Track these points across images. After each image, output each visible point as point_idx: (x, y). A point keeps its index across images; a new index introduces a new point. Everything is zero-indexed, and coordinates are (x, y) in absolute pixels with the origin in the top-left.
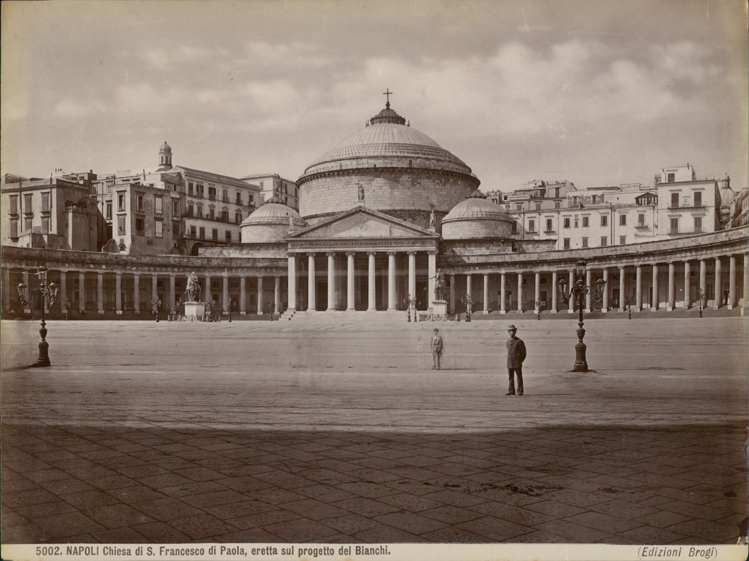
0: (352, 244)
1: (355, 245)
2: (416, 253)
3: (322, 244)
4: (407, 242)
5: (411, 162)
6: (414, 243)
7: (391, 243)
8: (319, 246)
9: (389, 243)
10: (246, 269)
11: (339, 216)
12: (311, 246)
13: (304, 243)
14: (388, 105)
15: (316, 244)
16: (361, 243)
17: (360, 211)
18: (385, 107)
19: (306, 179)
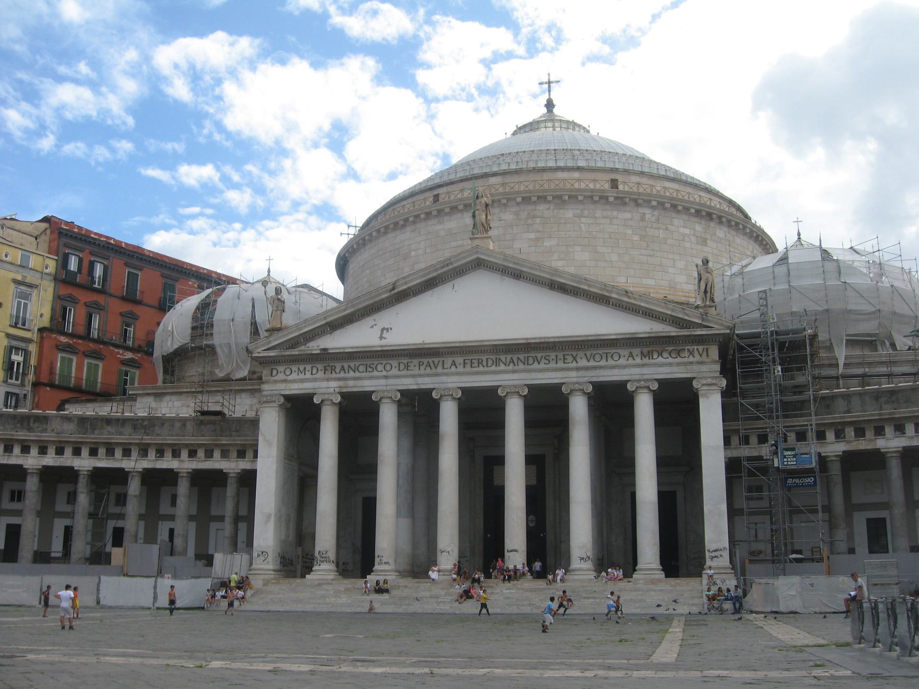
0: (454, 363)
1: (460, 369)
2: (655, 386)
3: (361, 368)
4: (624, 352)
5: (614, 184)
6: (649, 355)
7: (575, 359)
8: (352, 374)
9: (570, 359)
12: (328, 375)
13: (308, 367)
14: (550, 105)
15: (343, 369)
16: (480, 362)
17: (478, 264)
18: (545, 110)
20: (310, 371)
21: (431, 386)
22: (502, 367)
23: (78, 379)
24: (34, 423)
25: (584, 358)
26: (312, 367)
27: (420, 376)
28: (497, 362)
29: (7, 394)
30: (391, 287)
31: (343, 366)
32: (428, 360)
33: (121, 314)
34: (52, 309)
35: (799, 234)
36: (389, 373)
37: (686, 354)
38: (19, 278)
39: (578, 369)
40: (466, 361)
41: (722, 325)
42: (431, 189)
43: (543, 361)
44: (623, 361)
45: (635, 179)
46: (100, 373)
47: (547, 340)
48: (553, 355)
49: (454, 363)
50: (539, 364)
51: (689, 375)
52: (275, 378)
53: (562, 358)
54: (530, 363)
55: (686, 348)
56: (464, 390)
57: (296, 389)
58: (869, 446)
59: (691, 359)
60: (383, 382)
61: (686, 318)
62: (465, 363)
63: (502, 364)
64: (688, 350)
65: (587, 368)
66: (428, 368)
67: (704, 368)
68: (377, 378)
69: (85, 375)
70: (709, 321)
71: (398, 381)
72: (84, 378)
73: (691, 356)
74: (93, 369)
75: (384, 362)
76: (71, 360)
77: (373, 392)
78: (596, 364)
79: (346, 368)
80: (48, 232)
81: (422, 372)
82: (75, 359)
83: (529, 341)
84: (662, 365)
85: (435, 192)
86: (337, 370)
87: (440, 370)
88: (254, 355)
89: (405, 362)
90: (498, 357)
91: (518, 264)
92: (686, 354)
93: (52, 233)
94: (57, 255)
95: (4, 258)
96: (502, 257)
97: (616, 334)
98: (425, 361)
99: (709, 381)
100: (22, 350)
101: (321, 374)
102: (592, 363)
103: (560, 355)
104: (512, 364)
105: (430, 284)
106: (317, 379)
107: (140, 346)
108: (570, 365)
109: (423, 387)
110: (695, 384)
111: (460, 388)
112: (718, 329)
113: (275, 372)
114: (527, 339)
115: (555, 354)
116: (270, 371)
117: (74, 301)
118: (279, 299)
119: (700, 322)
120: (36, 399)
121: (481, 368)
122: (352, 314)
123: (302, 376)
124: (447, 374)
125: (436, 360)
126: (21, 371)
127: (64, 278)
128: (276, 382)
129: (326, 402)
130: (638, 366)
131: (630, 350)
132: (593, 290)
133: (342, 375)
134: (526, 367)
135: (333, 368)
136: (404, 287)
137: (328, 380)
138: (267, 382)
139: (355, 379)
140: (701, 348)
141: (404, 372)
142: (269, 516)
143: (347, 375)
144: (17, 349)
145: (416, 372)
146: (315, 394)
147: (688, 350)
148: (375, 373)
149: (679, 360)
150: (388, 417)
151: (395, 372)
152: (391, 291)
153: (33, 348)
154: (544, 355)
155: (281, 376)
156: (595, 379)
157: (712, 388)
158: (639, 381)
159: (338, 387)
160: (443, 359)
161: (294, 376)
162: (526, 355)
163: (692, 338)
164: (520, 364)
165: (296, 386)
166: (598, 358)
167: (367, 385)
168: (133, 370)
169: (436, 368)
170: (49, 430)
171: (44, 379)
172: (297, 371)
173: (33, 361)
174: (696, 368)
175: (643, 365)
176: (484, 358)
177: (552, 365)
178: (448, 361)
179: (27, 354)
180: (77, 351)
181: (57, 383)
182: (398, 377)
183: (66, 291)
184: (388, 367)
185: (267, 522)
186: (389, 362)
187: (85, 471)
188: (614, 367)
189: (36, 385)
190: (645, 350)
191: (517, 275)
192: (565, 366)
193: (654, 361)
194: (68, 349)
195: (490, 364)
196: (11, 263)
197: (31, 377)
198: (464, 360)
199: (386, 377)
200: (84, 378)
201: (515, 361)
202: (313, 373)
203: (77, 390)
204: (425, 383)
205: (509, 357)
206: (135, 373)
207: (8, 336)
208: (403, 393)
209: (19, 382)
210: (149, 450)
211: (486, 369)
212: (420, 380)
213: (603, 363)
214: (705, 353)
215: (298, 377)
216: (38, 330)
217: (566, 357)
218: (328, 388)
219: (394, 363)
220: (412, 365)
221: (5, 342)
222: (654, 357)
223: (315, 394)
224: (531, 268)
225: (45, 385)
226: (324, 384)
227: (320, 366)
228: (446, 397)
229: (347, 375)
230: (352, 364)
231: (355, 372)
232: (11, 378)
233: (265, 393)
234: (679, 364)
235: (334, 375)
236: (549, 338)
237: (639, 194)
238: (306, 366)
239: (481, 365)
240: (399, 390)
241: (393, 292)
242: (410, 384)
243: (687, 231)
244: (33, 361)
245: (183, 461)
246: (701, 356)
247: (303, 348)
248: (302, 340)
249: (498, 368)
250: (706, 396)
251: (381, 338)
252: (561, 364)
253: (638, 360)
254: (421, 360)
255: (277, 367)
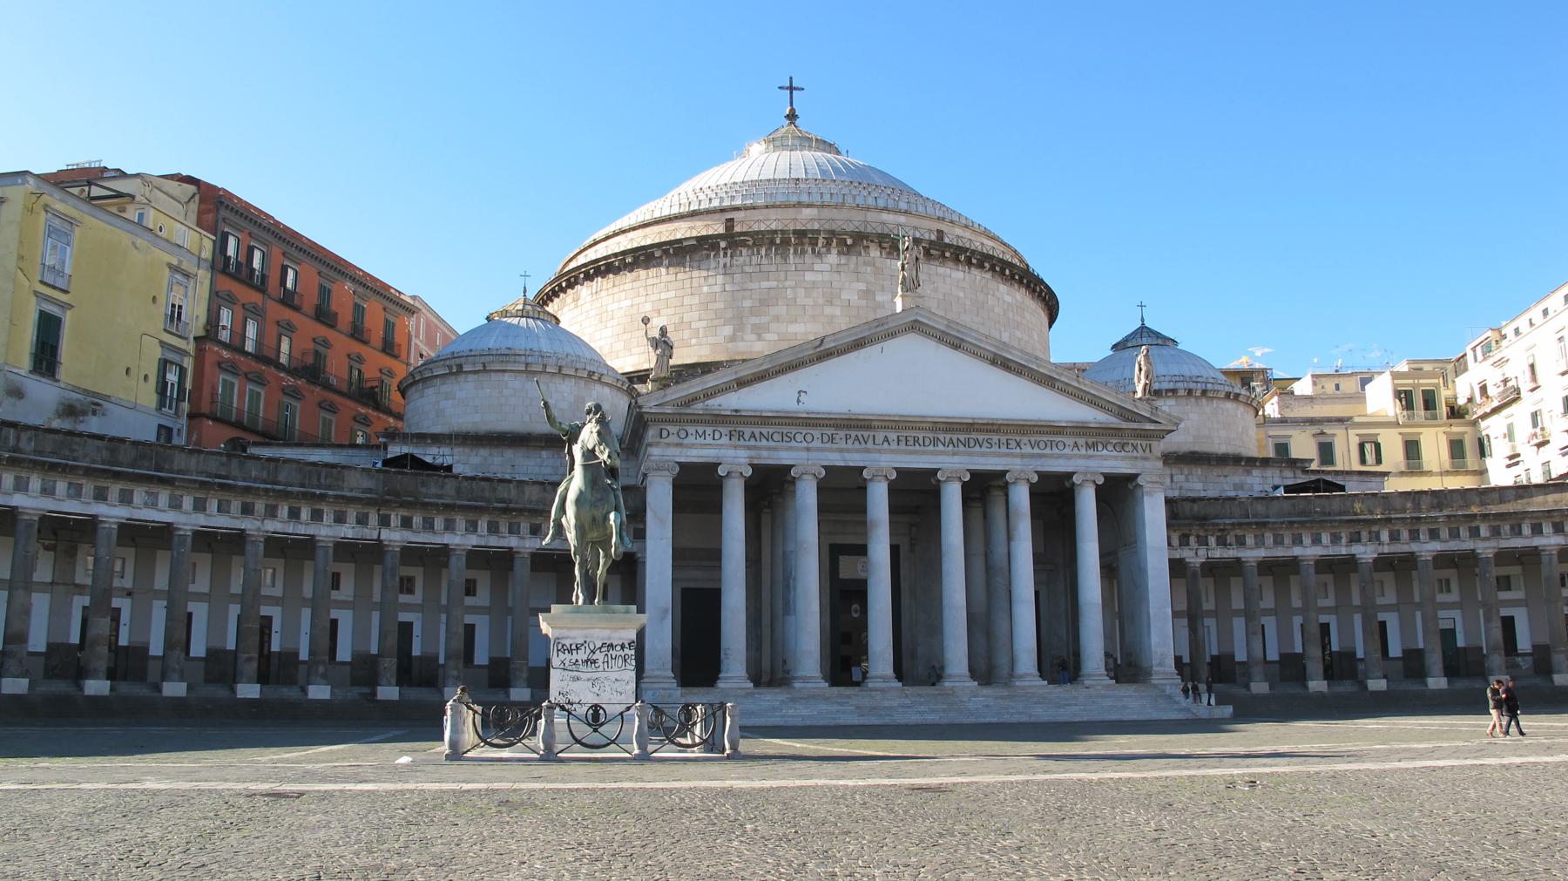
1: (894, 446)
2: (1101, 481)
3: (776, 437)
4: (1069, 441)
6: (1094, 446)
7: (1018, 444)
8: (764, 442)
9: (1013, 444)
10: (526, 514)
11: (745, 371)
12: (735, 441)
13: (709, 430)
16: (916, 440)
17: (916, 327)
19: (567, 280)
20: (712, 435)
21: (861, 464)
22: (941, 447)
23: (240, 411)
24: (326, 479)
25: (1028, 444)
26: (714, 431)
27: (848, 451)
28: (935, 442)
29: (160, 426)
30: (818, 343)
31: (753, 432)
32: (856, 433)
33: (278, 323)
34: (208, 310)
35: (1143, 320)
36: (810, 445)
37: (1130, 448)
38: (175, 262)
39: (1023, 456)
40: (900, 438)
41: (1170, 421)
42: (723, 211)
43: (985, 444)
44: (1067, 451)
45: (958, 231)
46: (262, 406)
47: (995, 422)
48: (995, 438)
49: (886, 439)
50: (981, 447)
51: (1133, 471)
52: (662, 440)
53: (1005, 442)
54: (972, 444)
55: (1130, 442)
56: (899, 471)
57: (697, 453)
58: (1290, 554)
59: (1135, 453)
60: (804, 455)
61: (1136, 410)
62: (899, 441)
63: (940, 444)
64: (1132, 444)
65: (1032, 456)
66: (857, 442)
67: (1147, 464)
68: (798, 449)
69: (246, 407)
70: (1158, 417)
71: (822, 455)
72: (246, 409)
73: (1135, 451)
74: (255, 397)
75: (804, 432)
76: (232, 384)
77: (793, 466)
78: (1040, 451)
79: (757, 435)
80: (197, 197)
81: (850, 445)
82: (236, 382)
83: (976, 421)
84: (1106, 458)
85: (729, 215)
86: (747, 436)
87: (870, 445)
88: (643, 410)
89: (829, 432)
90: (935, 435)
91: (962, 333)
92: (1130, 448)
93: (201, 201)
94: (215, 235)
95: (159, 233)
96: (946, 322)
97: (1067, 422)
98: (853, 434)
99: (1155, 479)
100: (176, 365)
101: (725, 440)
102: (1036, 451)
103: (1003, 439)
104: (951, 445)
105: (858, 345)
106: (722, 445)
107: (295, 369)
108: (1014, 451)
109: (851, 464)
110: (1140, 480)
111: (895, 468)
112: (1166, 425)
113: (665, 433)
114: (974, 419)
115: (998, 437)
116: (659, 432)
117: (230, 300)
118: (665, 342)
119: (1148, 416)
120: (195, 437)
121: (917, 447)
122: (766, 370)
123: (700, 440)
124: (879, 451)
125: (866, 434)
126: (175, 396)
127: (220, 265)
128: (668, 445)
129: (733, 475)
130: (1081, 457)
131: (1074, 440)
132: (1041, 370)
133: (753, 442)
134: (967, 449)
135: (741, 434)
136: (833, 345)
137: (735, 447)
138: (657, 444)
139: (769, 449)
140: (1144, 443)
141: (829, 445)
142: (666, 611)
143: (758, 443)
144: (172, 363)
145: (843, 445)
146: (720, 464)
147: (1132, 444)
148: (793, 443)
149: (1123, 453)
150: (807, 496)
151: (817, 444)
152: (816, 348)
153: (188, 363)
154: (986, 437)
155: (673, 439)
156: (1039, 469)
157: (1156, 485)
158: (1085, 474)
159: (749, 458)
160: (873, 433)
161: (691, 440)
162: (968, 436)
163: (1138, 432)
164: (960, 444)
165: (694, 452)
166: (1042, 445)
167: (783, 457)
168: (294, 403)
169: (866, 443)
170: (345, 489)
171: (205, 409)
172: (694, 434)
173: (188, 386)
174: (1140, 463)
175: (1090, 457)
176: (921, 435)
177: (995, 449)
178: (880, 436)
179: (182, 372)
180: (241, 373)
181: (218, 415)
182: (822, 450)
183: (227, 284)
184: (809, 438)
185: (663, 618)
186: (812, 432)
187: (397, 546)
188: (1059, 457)
189: (191, 416)
190: (1090, 441)
191: (957, 344)
192: (1008, 451)
193: (1096, 453)
194: (232, 369)
195: (927, 442)
196: (167, 241)
197: (186, 406)
198: (898, 437)
199: (808, 449)
200: (246, 409)
201: (955, 441)
202: (716, 438)
203: (238, 425)
204: (854, 460)
205: (948, 436)
206: (296, 407)
207: (163, 344)
208: (825, 467)
209: (173, 411)
210: (479, 523)
211: (922, 448)
212: (847, 456)
213: (1048, 451)
214: (1148, 448)
215: (695, 441)
216: (196, 339)
217: (1009, 442)
218: (735, 457)
219: (817, 433)
220: (837, 437)
221: (158, 353)
222: (1100, 449)
223: (720, 464)
224: (976, 339)
225: (208, 418)
226: (731, 452)
227: (724, 430)
228: (879, 478)
229: (758, 443)
230: (764, 431)
231: (768, 440)
232: (165, 407)
233: (653, 458)
234: (1124, 458)
235: (742, 442)
236: (997, 419)
237: (973, 252)
238: (704, 428)
239: (916, 444)
240: (823, 466)
241: (818, 350)
242: (836, 460)
243: (1008, 299)
244: (188, 386)
245: (524, 538)
246: (1144, 451)
247: (700, 405)
248: (702, 396)
249: (936, 448)
250: (1150, 494)
251: (798, 401)
252: (1004, 449)
253: (1083, 451)
254: (847, 432)
255: (669, 428)
